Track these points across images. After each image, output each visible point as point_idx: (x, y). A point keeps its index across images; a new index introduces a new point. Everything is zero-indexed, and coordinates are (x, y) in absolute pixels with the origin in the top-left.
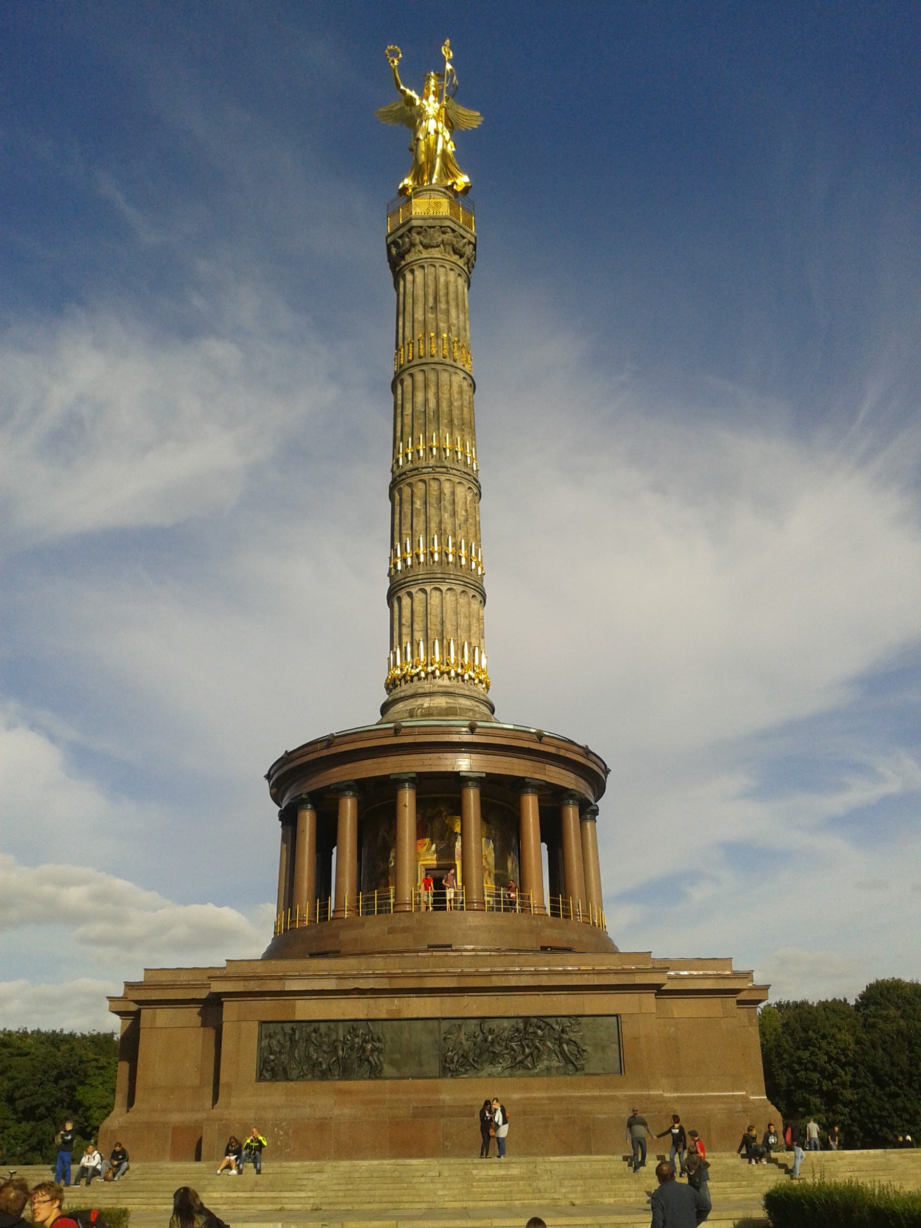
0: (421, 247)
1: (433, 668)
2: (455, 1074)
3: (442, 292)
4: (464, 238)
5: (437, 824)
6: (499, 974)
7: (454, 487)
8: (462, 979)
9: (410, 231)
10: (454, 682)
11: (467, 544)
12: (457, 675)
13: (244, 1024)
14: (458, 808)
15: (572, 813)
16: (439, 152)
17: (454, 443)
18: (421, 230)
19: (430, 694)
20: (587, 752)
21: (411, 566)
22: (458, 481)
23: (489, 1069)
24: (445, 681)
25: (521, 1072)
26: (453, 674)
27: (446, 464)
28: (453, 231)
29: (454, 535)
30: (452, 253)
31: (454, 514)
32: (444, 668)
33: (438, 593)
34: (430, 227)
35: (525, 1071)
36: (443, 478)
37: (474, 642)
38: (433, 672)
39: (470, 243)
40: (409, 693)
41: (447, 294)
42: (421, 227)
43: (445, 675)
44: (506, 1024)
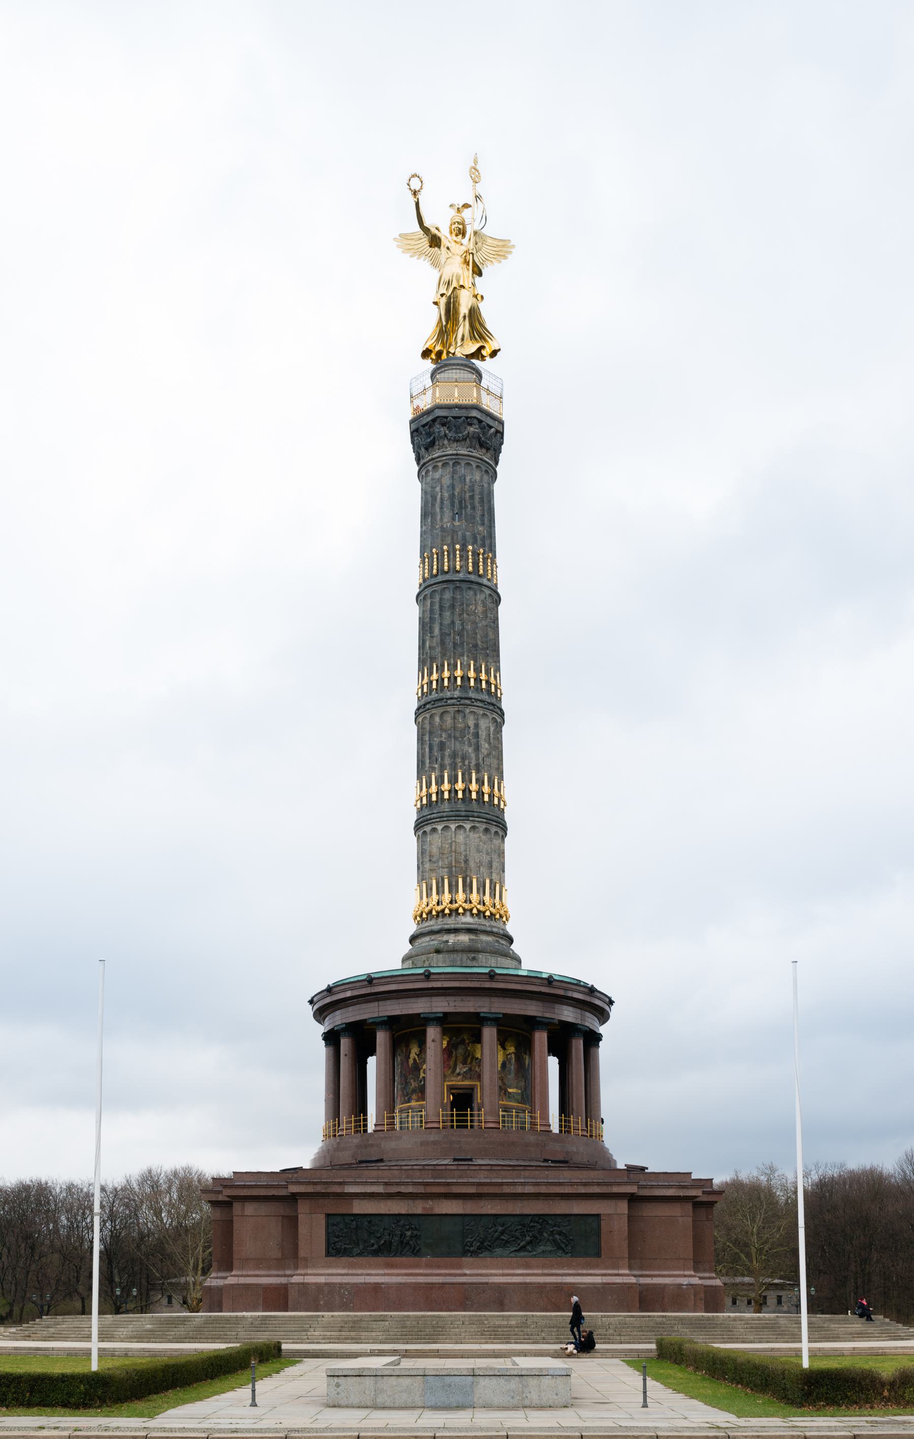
1: (457, 905)
2: (474, 1254)
4: (491, 427)
5: (461, 1050)
6: (508, 1184)
7: (477, 719)
8: (480, 1187)
9: (434, 420)
10: (476, 919)
11: (489, 778)
12: (478, 910)
13: (313, 1216)
14: (477, 1038)
15: (578, 1045)
16: (464, 310)
17: (478, 670)
19: (456, 931)
20: (592, 990)
21: (437, 802)
22: (481, 712)
23: (498, 1251)
24: (468, 919)
25: (522, 1254)
26: (475, 911)
27: (472, 694)
29: (478, 772)
30: (478, 446)
31: (477, 749)
32: (467, 906)
33: (462, 832)
35: (526, 1253)
36: (468, 711)
37: (495, 877)
38: (457, 909)
39: (497, 432)
40: (436, 928)
41: (472, 497)
43: (468, 913)
44: (512, 1219)
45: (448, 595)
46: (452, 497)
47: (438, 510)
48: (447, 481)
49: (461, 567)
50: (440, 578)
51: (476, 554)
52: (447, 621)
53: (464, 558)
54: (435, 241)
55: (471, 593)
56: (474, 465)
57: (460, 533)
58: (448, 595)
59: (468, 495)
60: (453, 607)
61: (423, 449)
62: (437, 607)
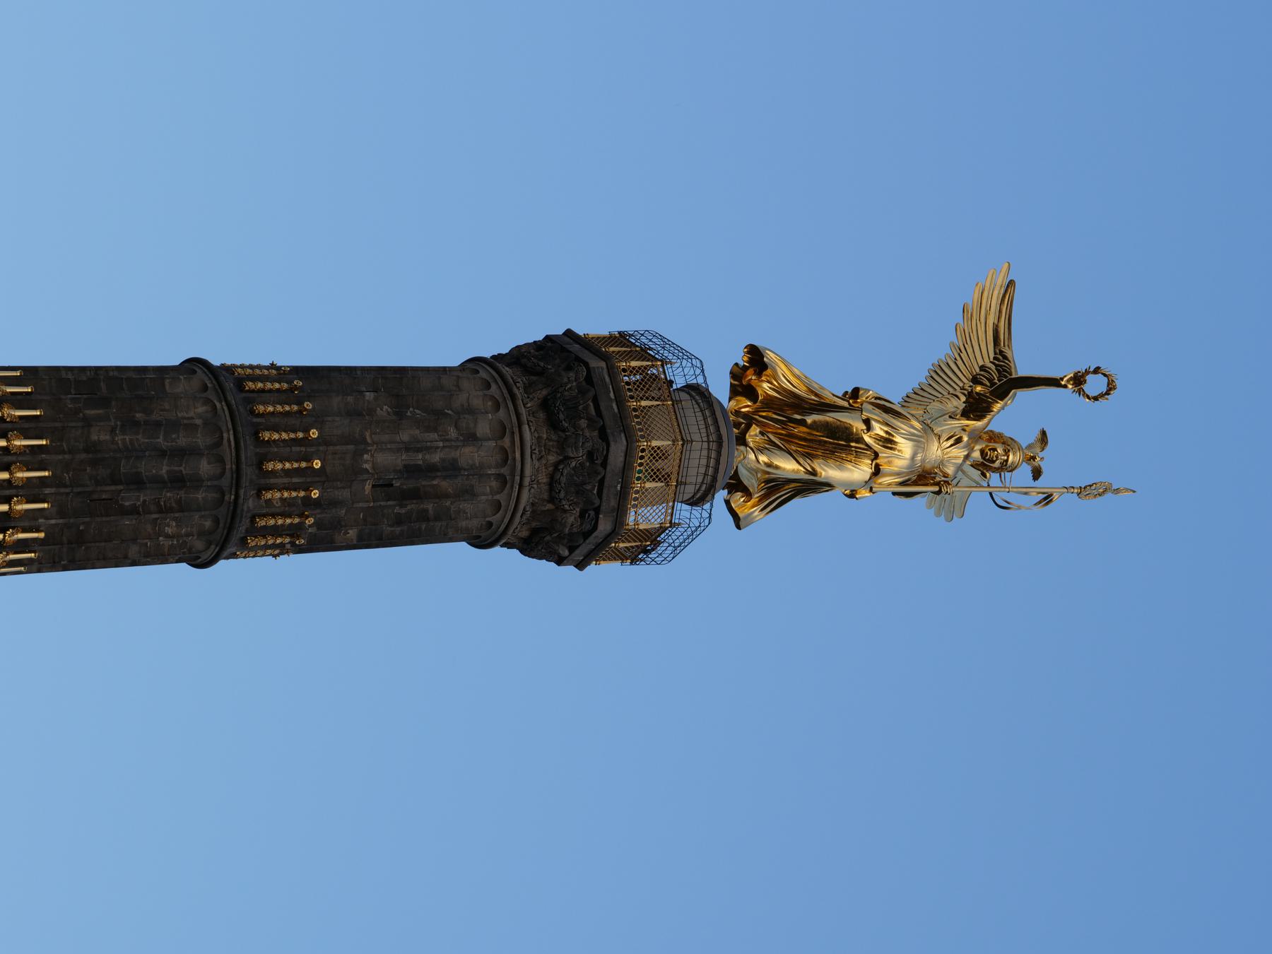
0: (552, 458)
3: (430, 507)
16: (829, 472)
18: (598, 459)
28: (586, 535)
30: (534, 524)
34: (601, 482)
42: (604, 464)
45: (205, 467)
46: (431, 470)
47: (405, 436)
48: (469, 455)
49: (269, 501)
50: (249, 452)
51: (294, 531)
52: (146, 468)
53: (288, 508)
54: (976, 407)
55: (208, 524)
56: (495, 519)
57: (345, 494)
58: (205, 467)
59: (430, 507)
60: (178, 481)
61: (545, 392)
62: (182, 441)
